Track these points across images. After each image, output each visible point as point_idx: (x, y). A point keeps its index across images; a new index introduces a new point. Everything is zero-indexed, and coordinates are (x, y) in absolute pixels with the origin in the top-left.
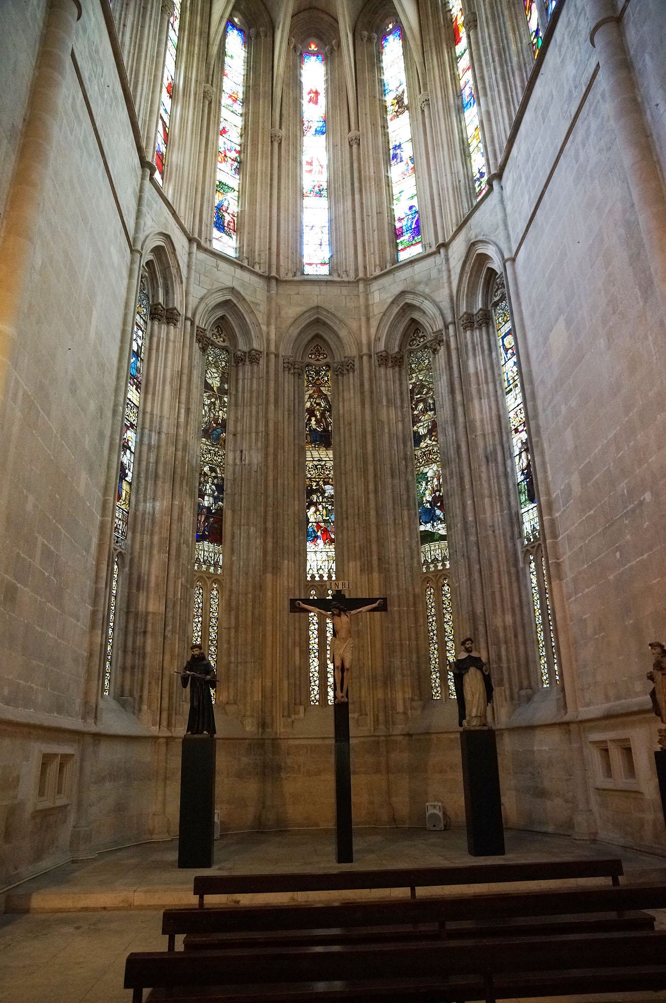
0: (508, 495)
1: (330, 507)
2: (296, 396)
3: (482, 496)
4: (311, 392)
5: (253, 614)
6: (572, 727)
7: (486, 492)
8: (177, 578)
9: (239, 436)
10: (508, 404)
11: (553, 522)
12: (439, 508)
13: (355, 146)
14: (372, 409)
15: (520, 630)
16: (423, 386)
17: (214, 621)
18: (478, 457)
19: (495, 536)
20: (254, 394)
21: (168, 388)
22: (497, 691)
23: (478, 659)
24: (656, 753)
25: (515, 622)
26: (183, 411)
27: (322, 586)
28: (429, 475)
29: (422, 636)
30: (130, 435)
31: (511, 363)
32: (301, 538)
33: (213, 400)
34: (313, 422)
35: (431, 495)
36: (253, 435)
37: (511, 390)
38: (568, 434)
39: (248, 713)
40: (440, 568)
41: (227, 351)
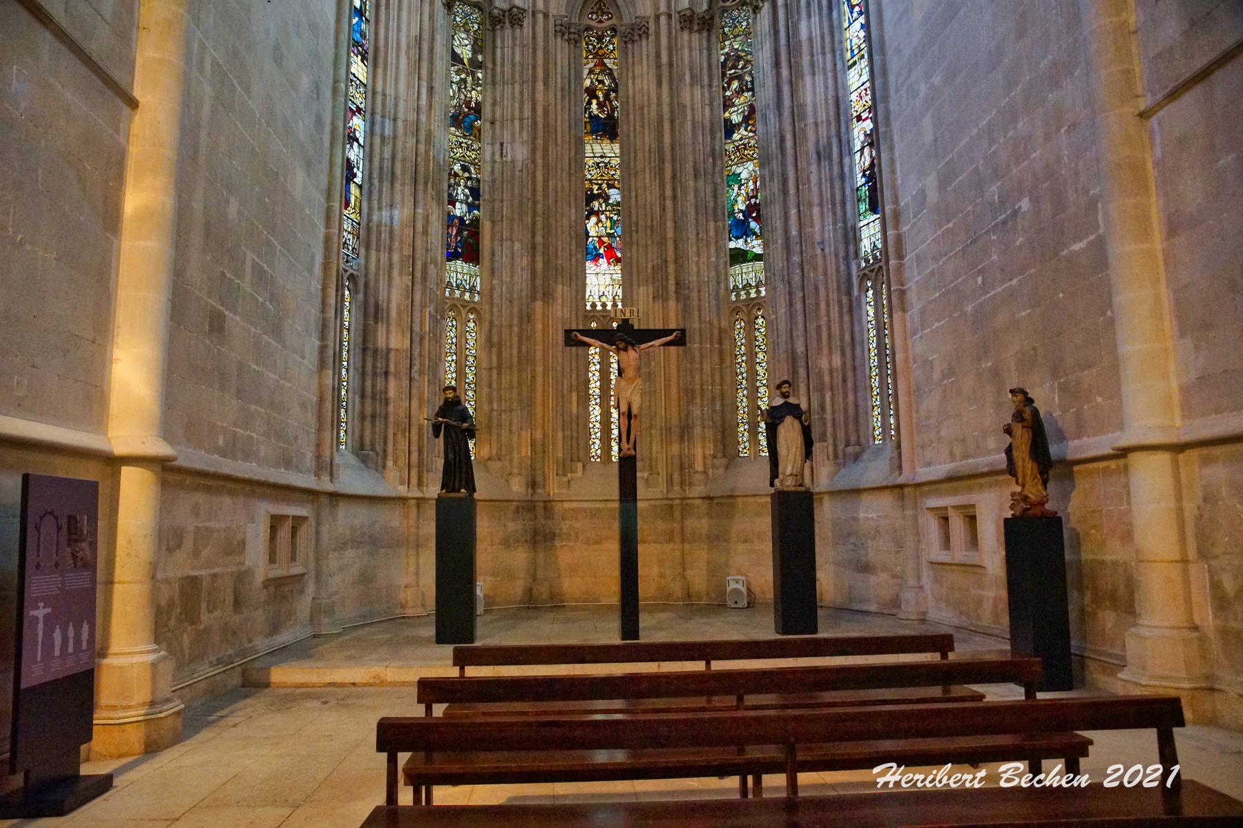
0: (844, 203)
1: (615, 218)
2: (572, 72)
3: (810, 205)
4: (591, 65)
5: (520, 351)
6: (907, 490)
7: (816, 201)
8: (423, 306)
9: (498, 125)
10: (850, 82)
11: (899, 239)
12: (755, 219)
14: (671, 89)
15: (849, 374)
16: (739, 58)
17: (471, 359)
18: (807, 153)
19: (824, 256)
20: (517, 68)
21: (403, 59)
22: (817, 447)
23: (798, 406)
24: (1006, 520)
25: (844, 364)
26: (424, 91)
27: (604, 317)
28: (742, 176)
29: (728, 380)
30: (357, 122)
31: (857, 25)
32: (579, 256)
33: (463, 76)
34: (594, 106)
36: (517, 123)
37: (855, 63)
38: (927, 121)
39: (516, 471)
40: (753, 295)
41: (480, 9)
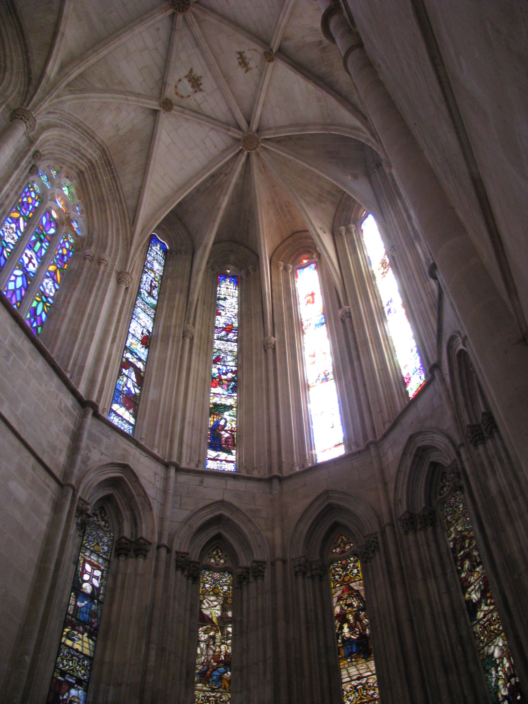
4: (339, 593)
13: (347, 320)
16: (464, 538)
28: (497, 654)
33: (212, 634)
34: (346, 630)
35: (505, 685)
41: (230, 573)
